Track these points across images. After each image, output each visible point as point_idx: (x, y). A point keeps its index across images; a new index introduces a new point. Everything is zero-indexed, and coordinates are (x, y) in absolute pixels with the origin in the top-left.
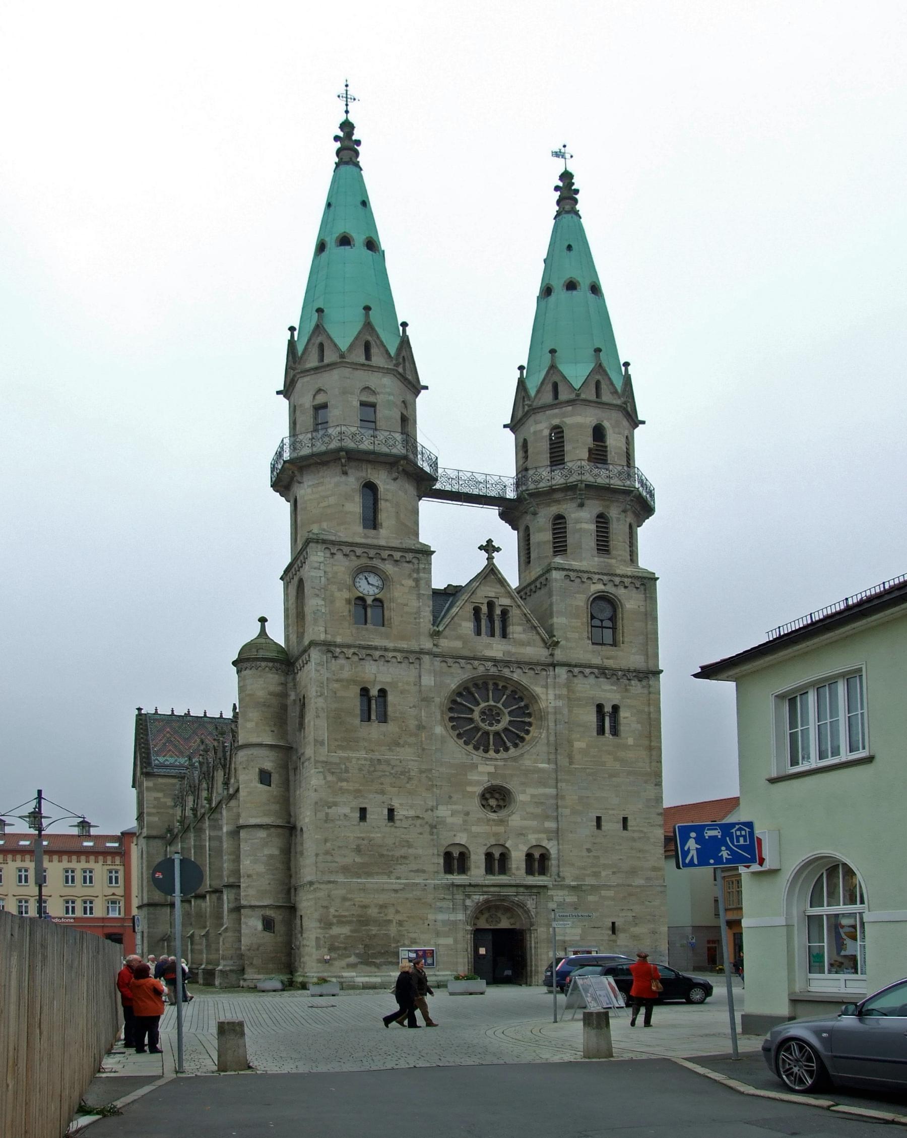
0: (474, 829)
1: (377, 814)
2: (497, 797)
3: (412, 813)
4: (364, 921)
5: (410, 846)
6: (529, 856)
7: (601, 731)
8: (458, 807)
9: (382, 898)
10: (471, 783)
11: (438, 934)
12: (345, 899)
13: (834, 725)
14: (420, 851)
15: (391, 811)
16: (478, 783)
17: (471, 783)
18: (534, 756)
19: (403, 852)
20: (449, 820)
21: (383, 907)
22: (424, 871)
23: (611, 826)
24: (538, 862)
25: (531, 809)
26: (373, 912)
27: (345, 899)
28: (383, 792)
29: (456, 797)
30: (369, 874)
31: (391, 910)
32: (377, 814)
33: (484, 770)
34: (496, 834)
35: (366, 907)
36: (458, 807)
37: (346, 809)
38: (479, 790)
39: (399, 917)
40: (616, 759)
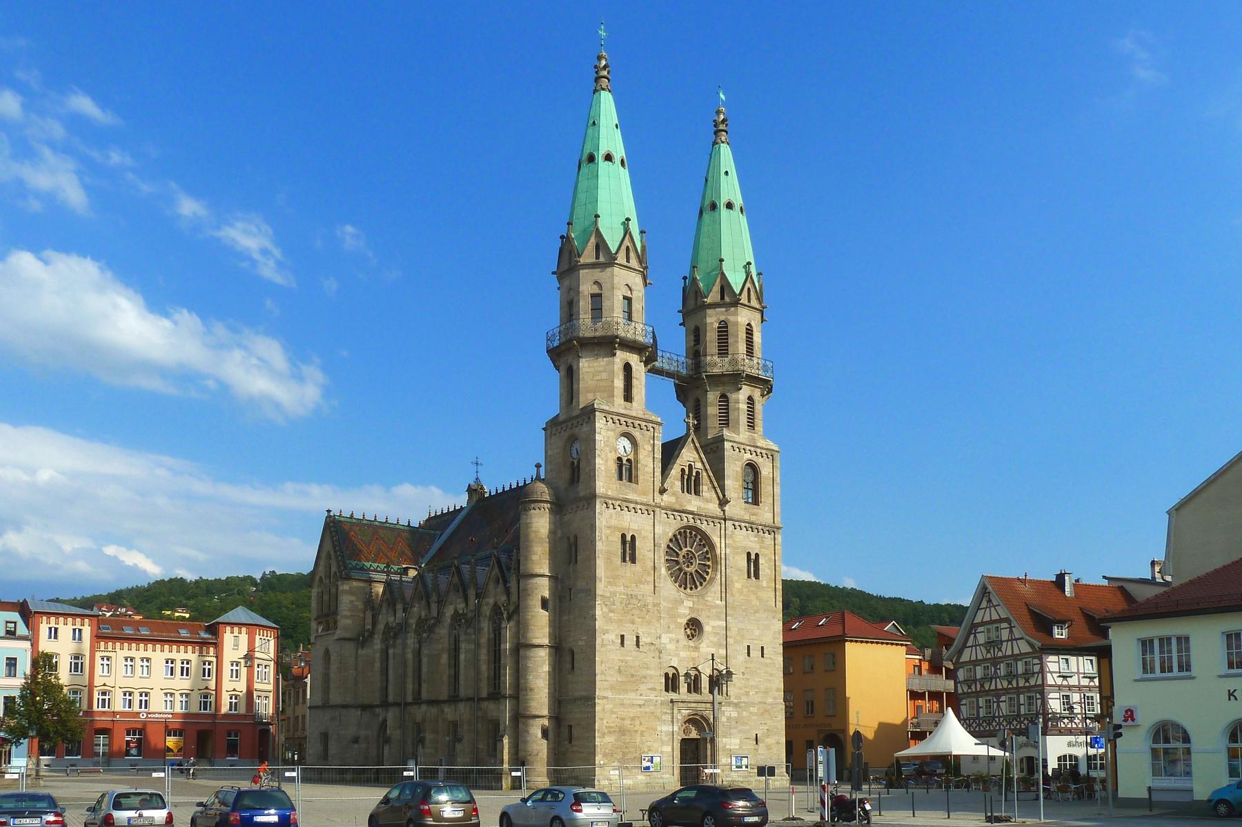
0: (683, 654)
1: (630, 641)
2: (694, 627)
3: (649, 640)
4: (622, 731)
5: (648, 668)
6: (711, 677)
7: (749, 577)
8: (673, 636)
9: (633, 711)
10: (679, 616)
11: (663, 743)
12: (612, 712)
13: (1170, 658)
14: (652, 672)
15: (638, 637)
16: (684, 615)
17: (679, 616)
18: (713, 594)
19: (644, 672)
20: (668, 646)
21: (633, 719)
22: (654, 689)
23: (755, 653)
24: (716, 682)
25: (712, 639)
26: (627, 722)
27: (612, 712)
28: (633, 622)
29: (672, 626)
30: (626, 691)
31: (637, 722)
32: (630, 641)
33: (687, 606)
34: (693, 659)
35: (623, 719)
36: (673, 636)
37: (613, 637)
38: (684, 621)
39: (642, 728)
40: (758, 598)
